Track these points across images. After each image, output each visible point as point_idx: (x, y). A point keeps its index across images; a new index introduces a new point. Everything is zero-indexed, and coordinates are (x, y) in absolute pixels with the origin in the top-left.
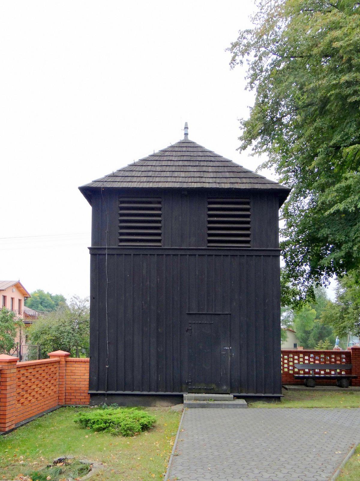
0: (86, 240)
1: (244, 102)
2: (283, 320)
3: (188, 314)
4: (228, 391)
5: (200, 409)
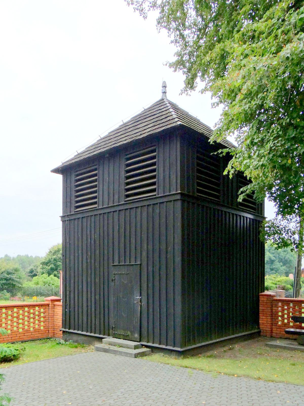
0: (60, 211)
1: (164, 46)
2: (267, 261)
3: (113, 266)
4: (138, 340)
5: (104, 353)
